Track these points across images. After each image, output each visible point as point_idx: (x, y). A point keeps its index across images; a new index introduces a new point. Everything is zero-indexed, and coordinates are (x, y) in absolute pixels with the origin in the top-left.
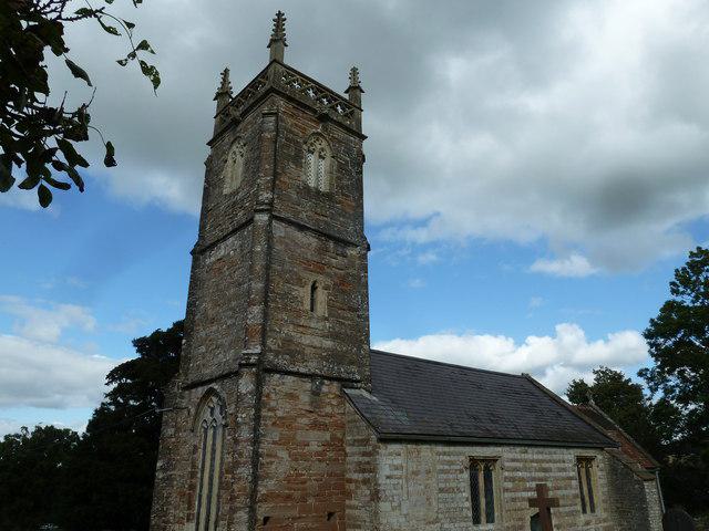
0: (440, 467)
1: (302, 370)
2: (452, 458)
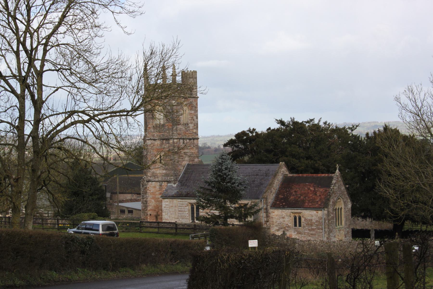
0: (179, 205)
1: (157, 180)
2: (183, 203)
